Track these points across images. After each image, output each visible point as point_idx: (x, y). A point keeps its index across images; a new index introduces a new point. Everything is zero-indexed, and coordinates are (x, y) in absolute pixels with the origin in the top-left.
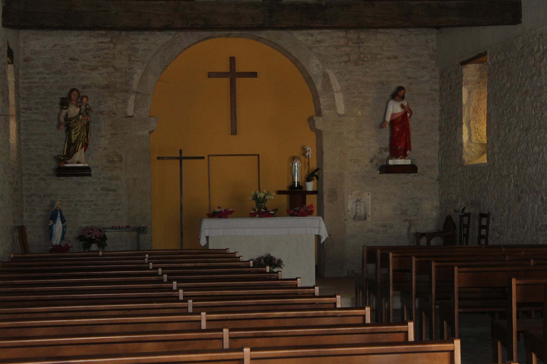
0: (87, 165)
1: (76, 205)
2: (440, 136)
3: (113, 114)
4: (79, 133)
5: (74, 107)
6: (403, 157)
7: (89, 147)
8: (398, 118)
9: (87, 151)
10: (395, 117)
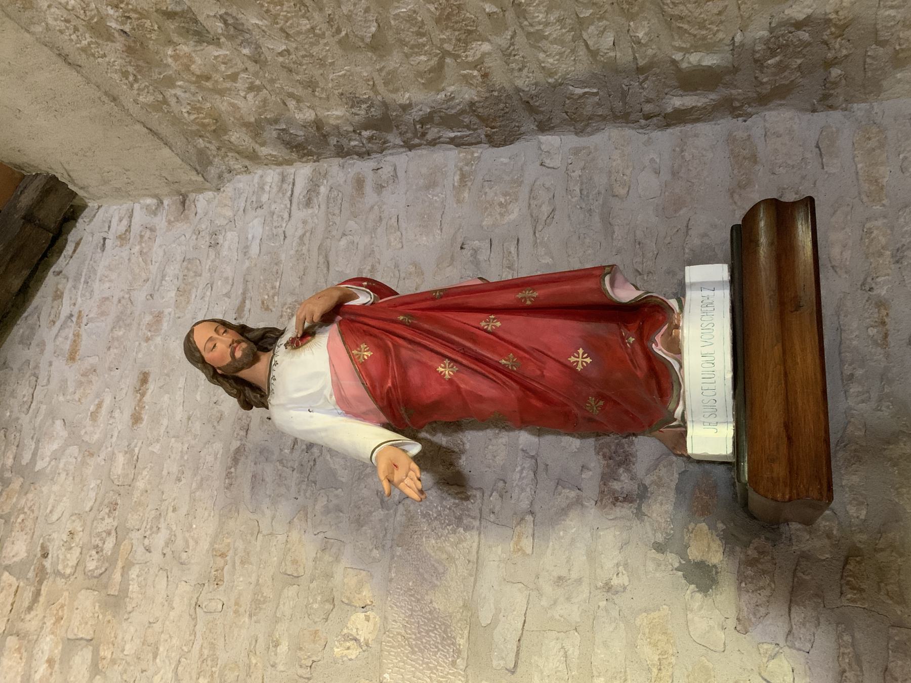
2: (544, 127)
6: (658, 338)
8: (362, 369)
10: (354, 387)
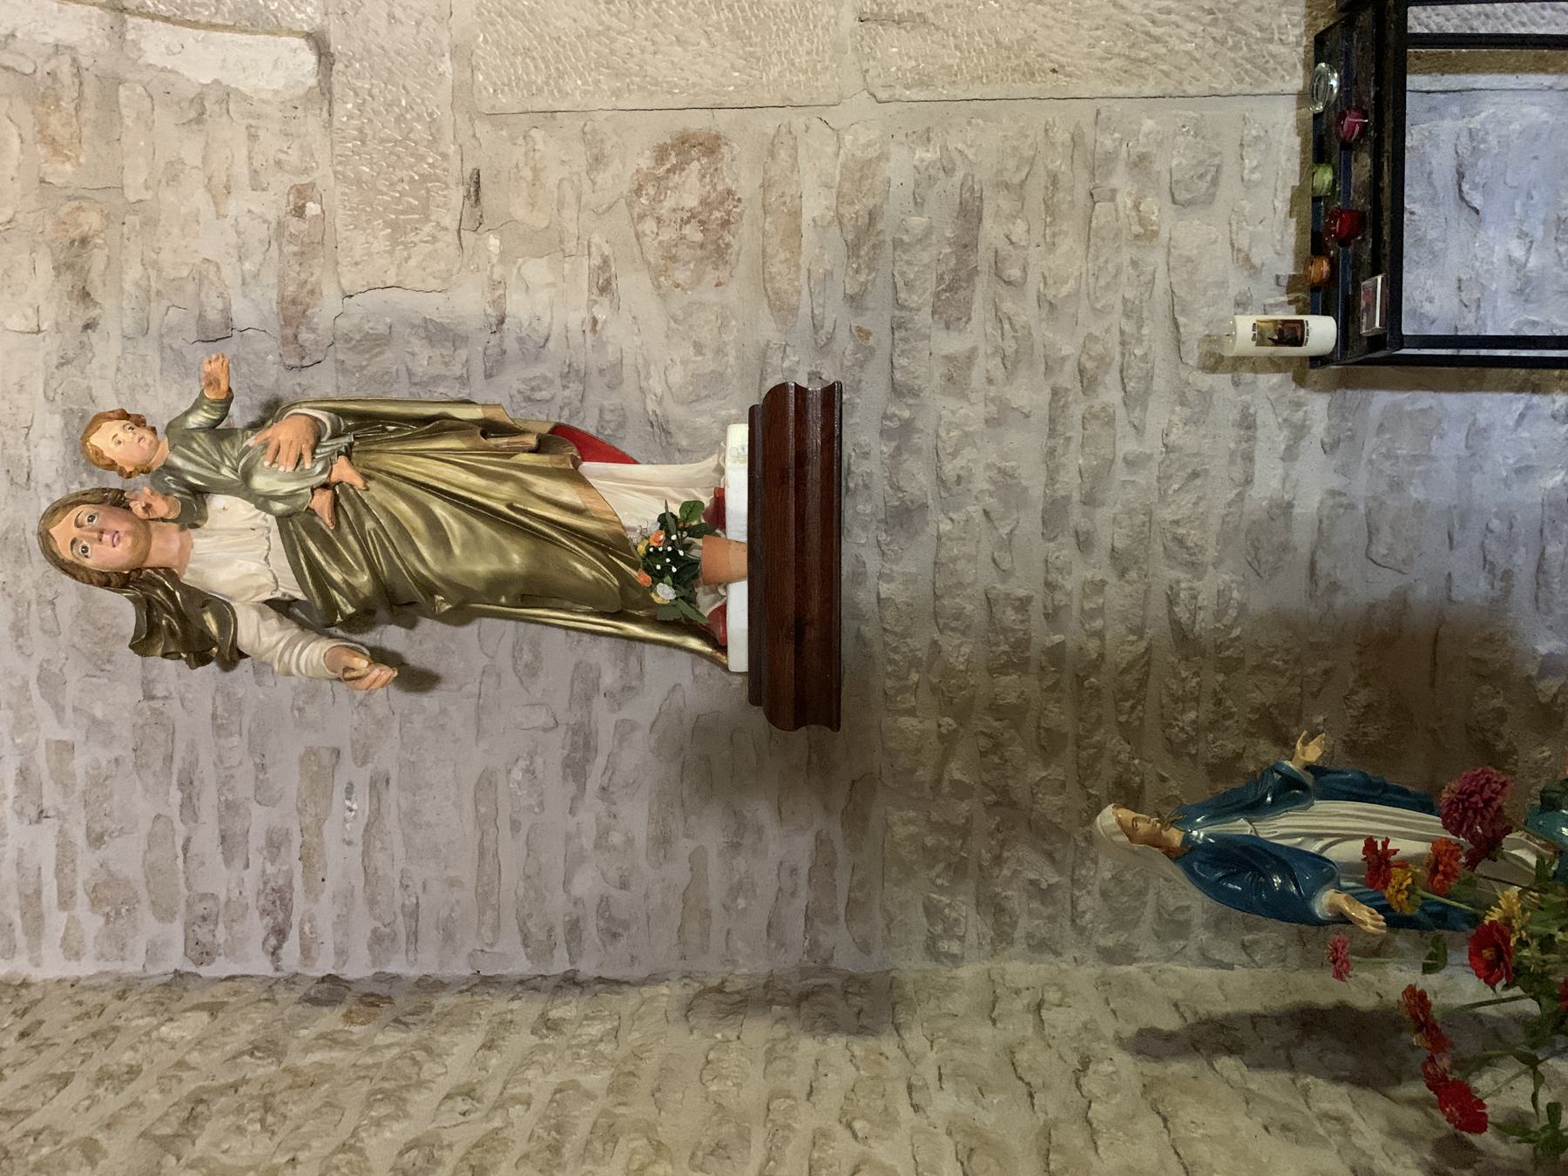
0: (739, 436)
1: (1084, 542)
3: (299, 212)
4: (440, 509)
5: (202, 544)
7: (589, 426)
9: (626, 448)
